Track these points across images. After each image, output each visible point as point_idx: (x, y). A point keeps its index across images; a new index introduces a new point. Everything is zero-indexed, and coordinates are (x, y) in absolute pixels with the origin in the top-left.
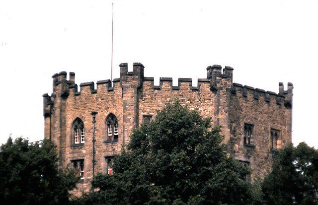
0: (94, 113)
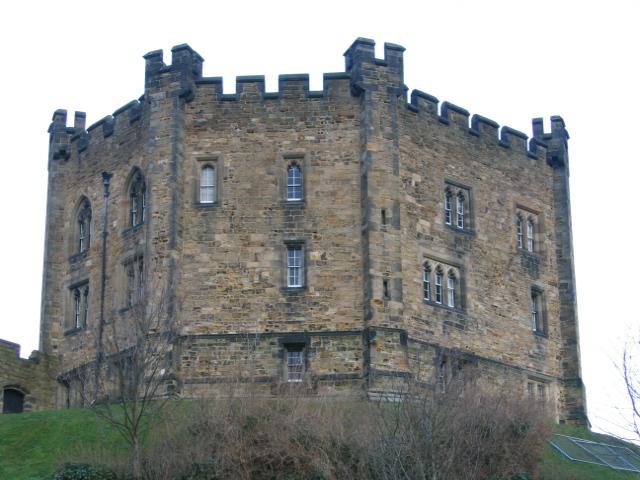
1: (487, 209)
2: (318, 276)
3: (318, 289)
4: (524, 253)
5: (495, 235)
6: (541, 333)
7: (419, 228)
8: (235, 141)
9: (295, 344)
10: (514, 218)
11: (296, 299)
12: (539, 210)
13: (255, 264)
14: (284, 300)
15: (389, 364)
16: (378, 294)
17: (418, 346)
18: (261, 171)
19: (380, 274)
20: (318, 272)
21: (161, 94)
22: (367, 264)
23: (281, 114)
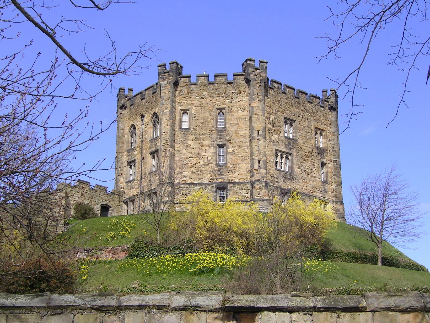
1: (302, 129)
4: (318, 148)
5: (306, 140)
7: (273, 138)
8: (196, 102)
9: (222, 188)
10: (314, 133)
11: (222, 169)
12: (324, 129)
13: (205, 154)
14: (217, 169)
15: (260, 195)
16: (256, 166)
17: (272, 188)
18: (207, 115)
19: (257, 158)
20: (231, 157)
21: (165, 82)
22: (252, 154)
23: (216, 90)
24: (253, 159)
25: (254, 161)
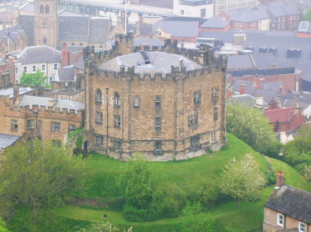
0: (107, 89)
2: (164, 126)
3: (164, 129)
6: (215, 118)
7: (187, 109)
13: (149, 123)
14: (155, 132)
18: (150, 99)
24: (177, 129)
25: (177, 130)
